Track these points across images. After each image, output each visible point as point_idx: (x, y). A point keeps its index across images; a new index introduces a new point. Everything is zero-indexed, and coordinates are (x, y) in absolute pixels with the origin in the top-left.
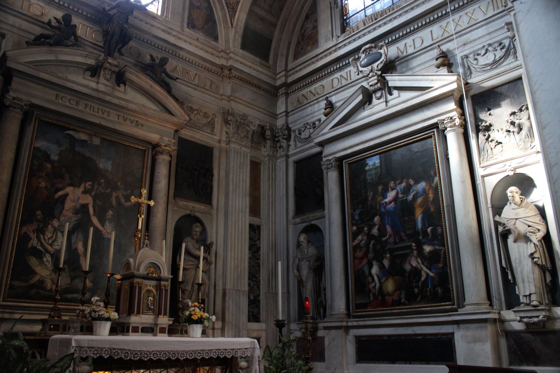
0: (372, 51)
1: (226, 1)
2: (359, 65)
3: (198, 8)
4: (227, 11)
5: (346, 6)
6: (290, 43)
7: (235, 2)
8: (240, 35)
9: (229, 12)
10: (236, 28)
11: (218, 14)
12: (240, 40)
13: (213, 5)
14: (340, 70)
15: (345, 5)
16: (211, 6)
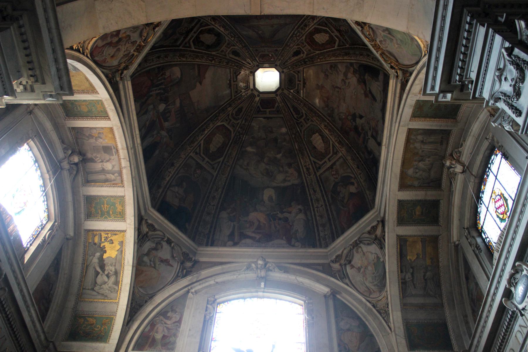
0: (517, 279)
1: (377, 309)
2: (516, 304)
3: (349, 330)
4: (381, 318)
5: (489, 244)
6: (466, 316)
7: (385, 305)
8: (402, 336)
9: (383, 318)
10: (395, 331)
11: (373, 325)
12: (404, 342)
13: (364, 320)
14: (515, 320)
15: (488, 243)
16: (363, 321)
